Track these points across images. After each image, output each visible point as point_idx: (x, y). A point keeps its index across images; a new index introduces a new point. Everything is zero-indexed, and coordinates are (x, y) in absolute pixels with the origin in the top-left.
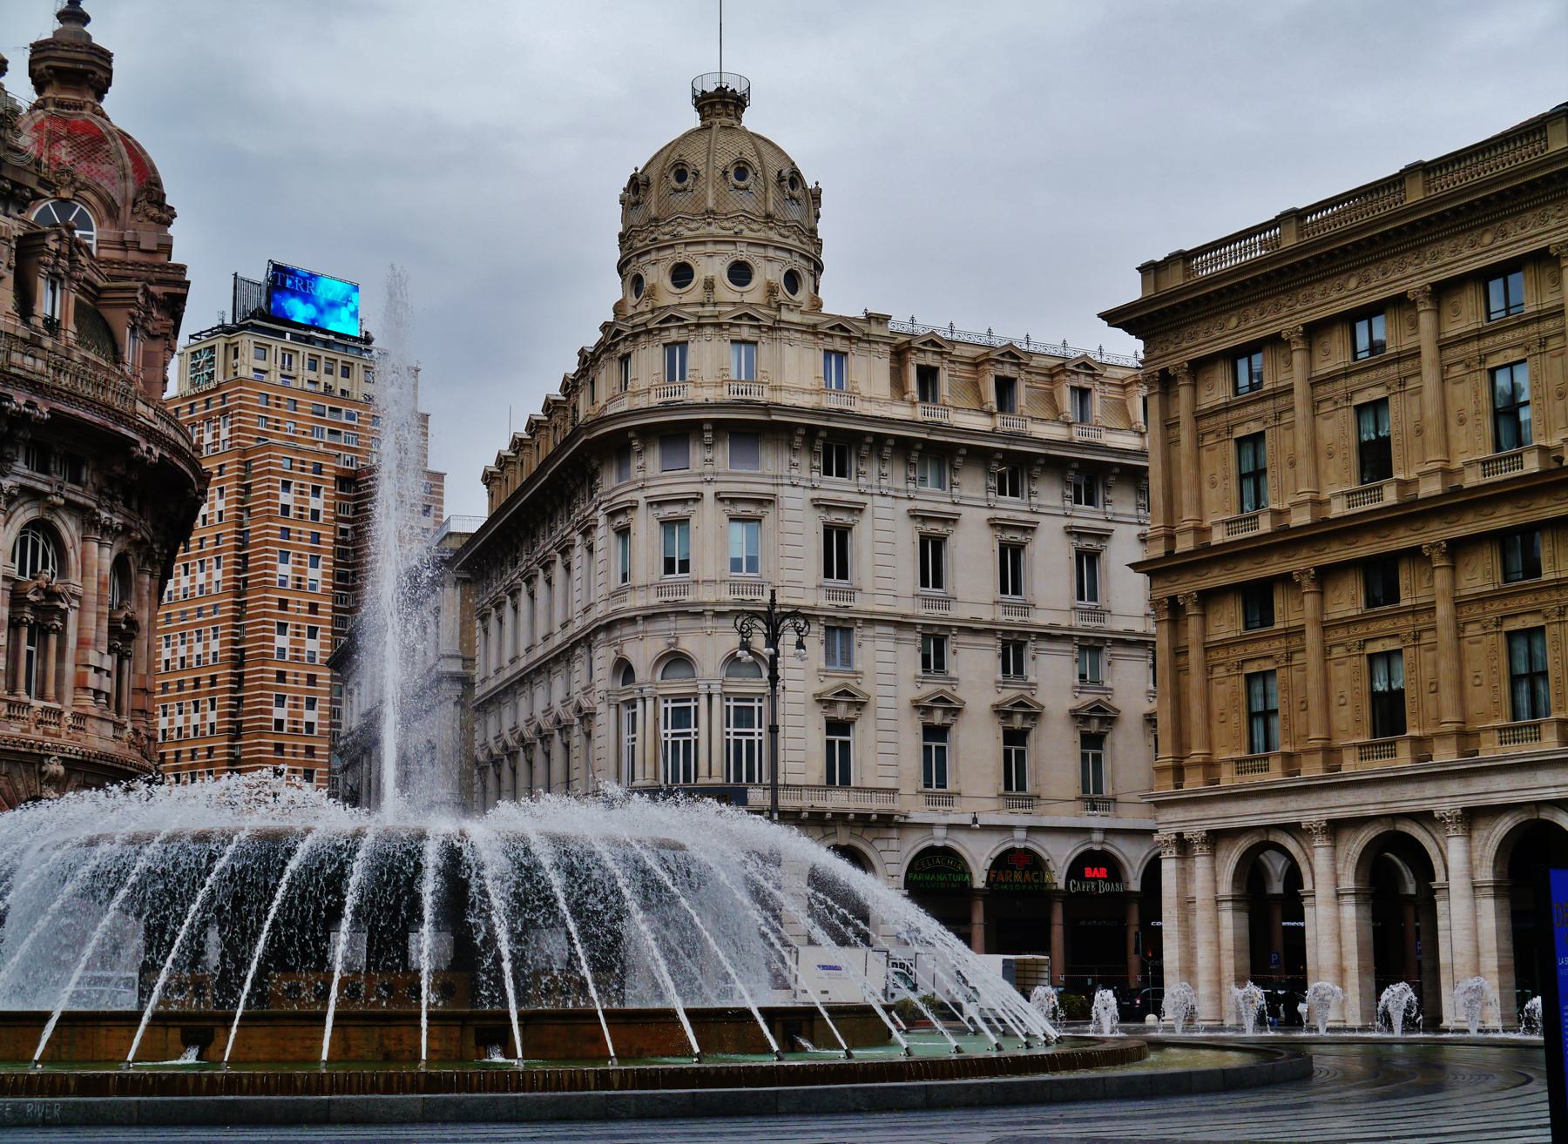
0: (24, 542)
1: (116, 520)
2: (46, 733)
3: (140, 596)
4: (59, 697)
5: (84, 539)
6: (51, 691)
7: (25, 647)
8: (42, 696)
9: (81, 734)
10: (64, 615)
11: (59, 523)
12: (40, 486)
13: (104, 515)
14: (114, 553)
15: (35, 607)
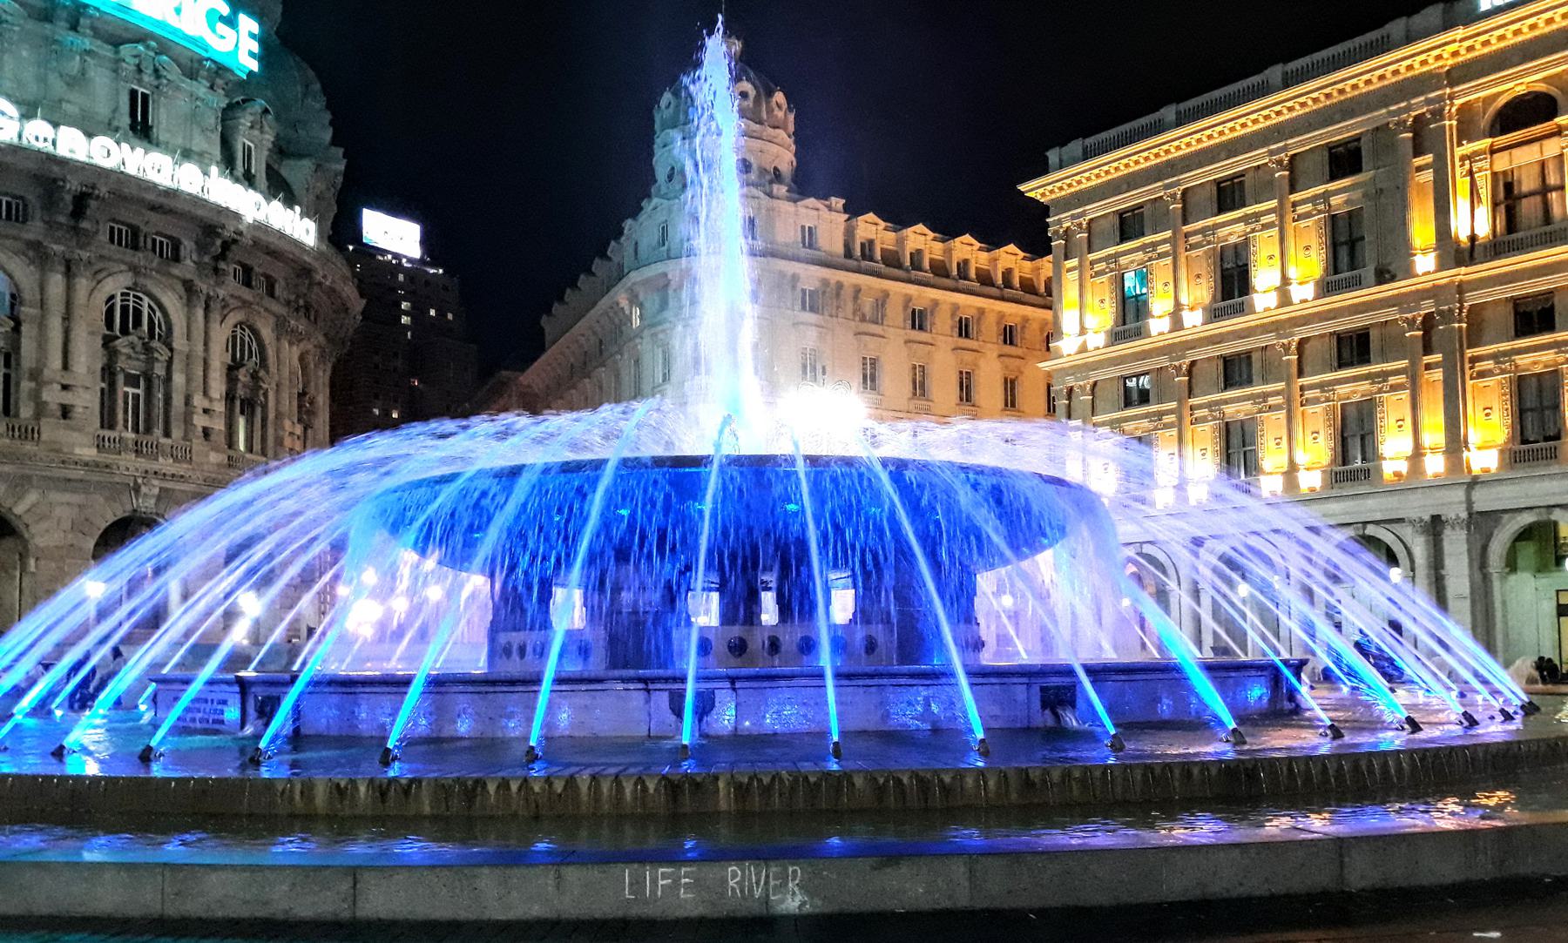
0: (234, 338)
5: (278, 339)
6: (257, 446)
10: (266, 395)
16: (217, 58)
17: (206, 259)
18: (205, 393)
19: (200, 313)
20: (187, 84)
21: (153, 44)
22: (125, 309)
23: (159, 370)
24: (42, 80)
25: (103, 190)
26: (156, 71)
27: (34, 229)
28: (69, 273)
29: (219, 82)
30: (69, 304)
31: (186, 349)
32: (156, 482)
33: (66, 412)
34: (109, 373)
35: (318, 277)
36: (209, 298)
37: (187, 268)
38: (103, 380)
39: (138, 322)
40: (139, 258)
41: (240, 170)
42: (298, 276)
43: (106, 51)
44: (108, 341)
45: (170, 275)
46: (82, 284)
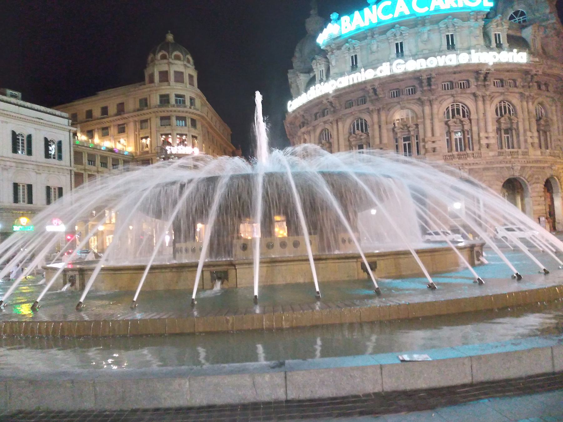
0: (501, 108)
1: (532, 94)
2: (512, 158)
3: (552, 113)
4: (519, 148)
5: (521, 101)
6: (515, 146)
7: (503, 135)
8: (513, 148)
9: (527, 157)
10: (517, 123)
11: (510, 98)
12: (500, 91)
13: (527, 94)
14: (536, 103)
15: (504, 123)
16: (474, 9)
17: (479, 83)
18: (486, 132)
19: (480, 103)
20: (466, 24)
21: (450, 17)
22: (453, 110)
23: (467, 127)
24: (417, 46)
25: (434, 75)
26: (453, 25)
27: (418, 95)
28: (431, 105)
29: (479, 17)
30: (432, 114)
31: (476, 117)
32: (467, 167)
33: (434, 150)
34: (449, 133)
35: (534, 72)
36: (483, 97)
37: (473, 89)
38: (447, 136)
39: (458, 113)
40: (453, 92)
41: (494, 44)
42: (526, 75)
43: (436, 27)
44: (446, 123)
45: (465, 93)
46: (435, 107)
